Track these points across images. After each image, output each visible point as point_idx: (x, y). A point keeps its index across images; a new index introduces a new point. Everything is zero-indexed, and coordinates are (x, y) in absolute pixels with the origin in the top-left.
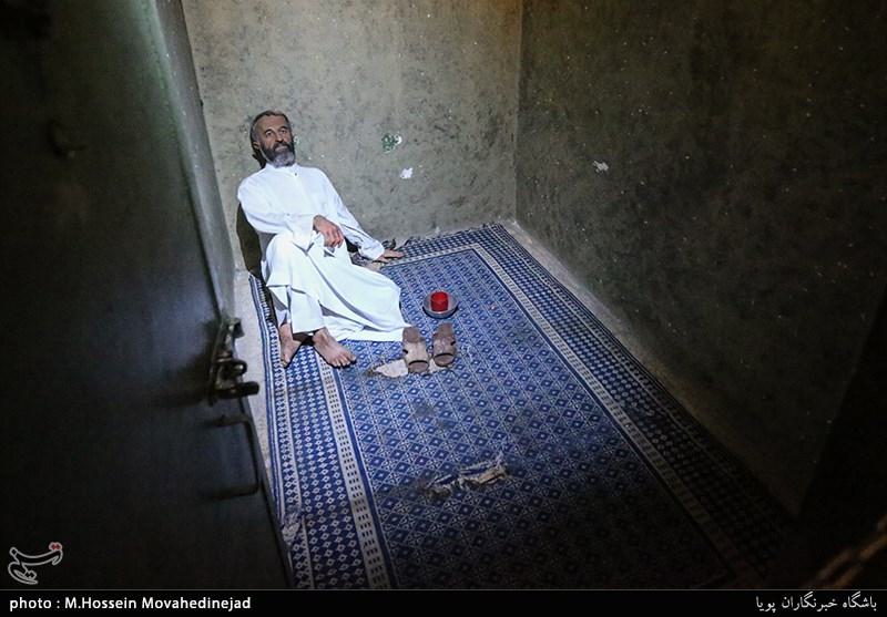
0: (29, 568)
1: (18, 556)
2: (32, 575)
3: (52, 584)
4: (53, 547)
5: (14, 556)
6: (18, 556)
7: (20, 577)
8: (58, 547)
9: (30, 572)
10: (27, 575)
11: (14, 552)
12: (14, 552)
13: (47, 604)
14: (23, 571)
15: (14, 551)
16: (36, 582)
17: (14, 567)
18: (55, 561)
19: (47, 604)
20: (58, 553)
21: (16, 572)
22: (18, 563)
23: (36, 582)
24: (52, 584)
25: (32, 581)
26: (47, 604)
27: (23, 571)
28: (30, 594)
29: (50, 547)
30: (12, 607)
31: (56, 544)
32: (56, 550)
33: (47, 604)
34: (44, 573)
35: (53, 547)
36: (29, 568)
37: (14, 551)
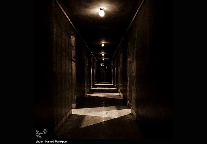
1: (38, 132)
3: (44, 137)
6: (38, 132)
10: (40, 136)
13: (41, 142)
14: (39, 135)
15: (37, 131)
17: (37, 134)
19: (41, 142)
22: (39, 134)
24: (44, 137)
25: (41, 137)
27: (39, 135)
28: (39, 139)
36: (40, 134)
37: (37, 131)
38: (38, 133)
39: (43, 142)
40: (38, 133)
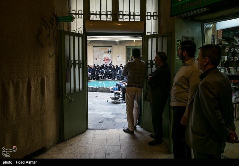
0: (8, 153)
1: (5, 150)
2: (8, 155)
4: (14, 147)
5: (4, 150)
6: (5, 150)
7: (5, 155)
8: (15, 147)
9: (8, 154)
10: (7, 155)
11: (3, 148)
12: (3, 148)
14: (6, 154)
16: (10, 157)
17: (3, 153)
18: (15, 151)
20: (15, 149)
21: (4, 154)
23: (10, 157)
25: (8, 156)
26: (11, 162)
27: (6, 154)
28: (7, 160)
29: (13, 147)
30: (3, 163)
31: (15, 146)
32: (15, 148)
33: (11, 162)
34: (12, 154)
35: (14, 147)
36: (8, 153)
37: (3, 148)
38: (6, 150)
39: (13, 163)
40: (6, 150)
